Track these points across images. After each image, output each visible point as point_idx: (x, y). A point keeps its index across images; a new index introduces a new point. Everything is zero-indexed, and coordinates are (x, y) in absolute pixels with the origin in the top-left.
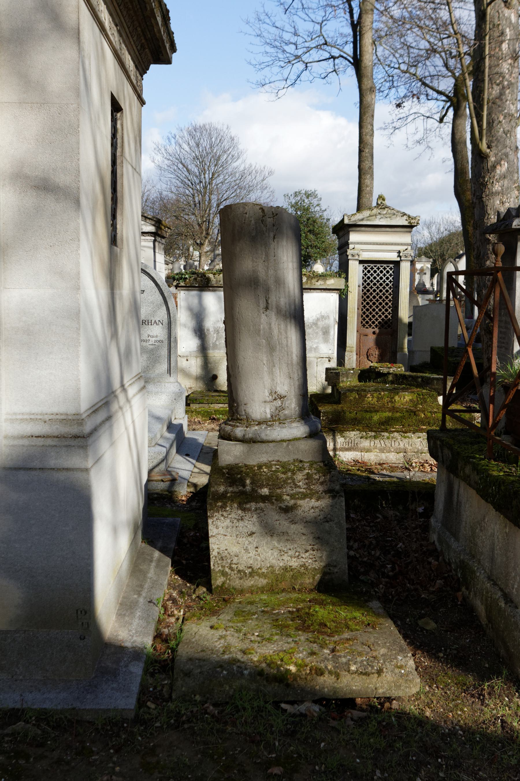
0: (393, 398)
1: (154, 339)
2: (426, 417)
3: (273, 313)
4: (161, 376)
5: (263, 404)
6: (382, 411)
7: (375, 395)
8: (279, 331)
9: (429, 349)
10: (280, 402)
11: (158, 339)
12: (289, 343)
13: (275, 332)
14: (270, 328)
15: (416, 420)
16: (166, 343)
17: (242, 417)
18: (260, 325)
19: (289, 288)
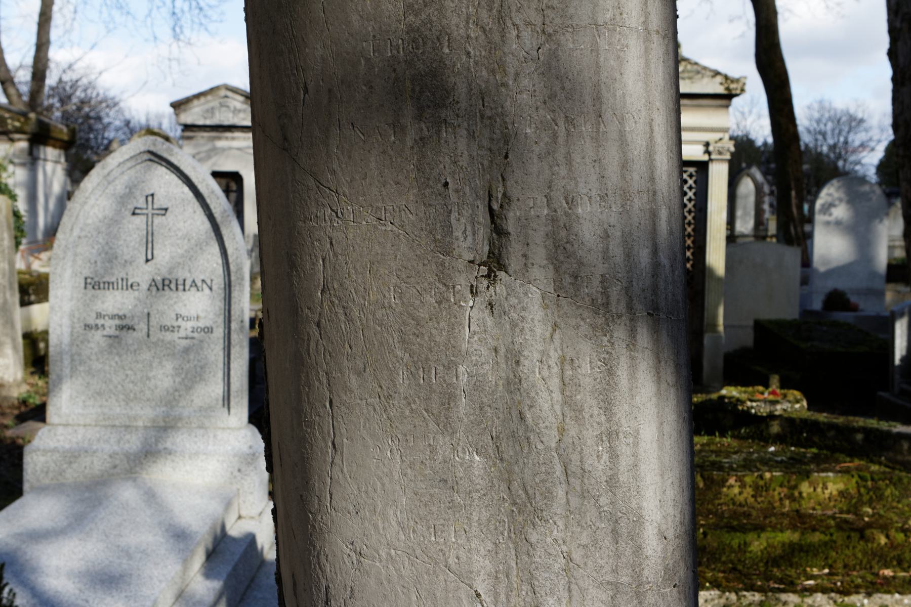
0: (795, 487)
2: (892, 546)
3: (535, 293)
4: (206, 411)
6: (774, 528)
7: (748, 480)
8: (567, 401)
9: (751, 323)
11: (201, 324)
12: (624, 463)
13: (547, 402)
14: (514, 383)
15: (865, 553)
16: (219, 332)
18: (451, 366)
19: (623, 141)
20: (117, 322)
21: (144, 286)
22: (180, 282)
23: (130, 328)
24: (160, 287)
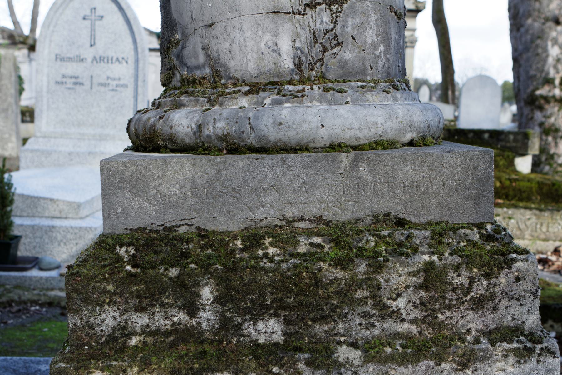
1: (115, 83)
5: (267, 22)
10: (326, 17)
11: (121, 82)
17: (198, 74)
20: (74, 80)
21: (89, 60)
22: (110, 58)
23: (81, 84)
24: (98, 60)
